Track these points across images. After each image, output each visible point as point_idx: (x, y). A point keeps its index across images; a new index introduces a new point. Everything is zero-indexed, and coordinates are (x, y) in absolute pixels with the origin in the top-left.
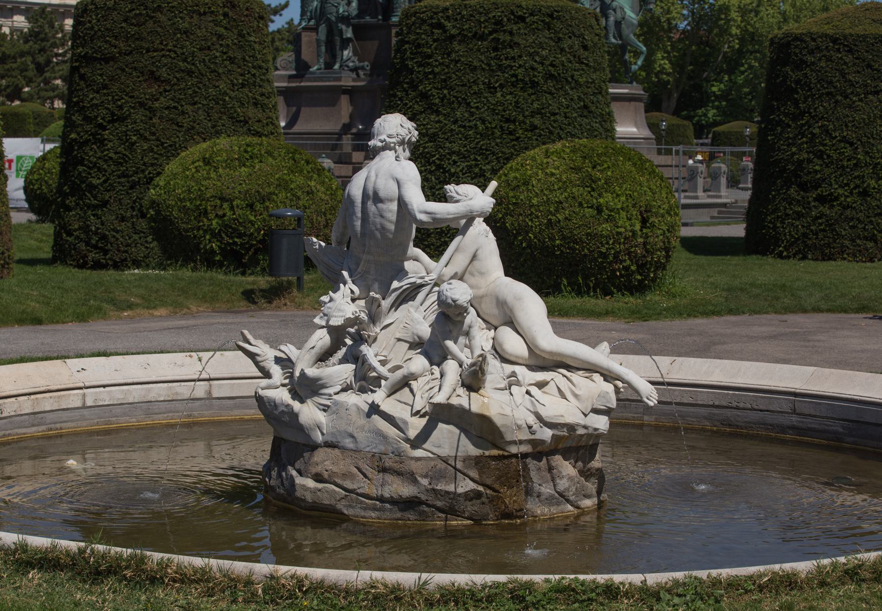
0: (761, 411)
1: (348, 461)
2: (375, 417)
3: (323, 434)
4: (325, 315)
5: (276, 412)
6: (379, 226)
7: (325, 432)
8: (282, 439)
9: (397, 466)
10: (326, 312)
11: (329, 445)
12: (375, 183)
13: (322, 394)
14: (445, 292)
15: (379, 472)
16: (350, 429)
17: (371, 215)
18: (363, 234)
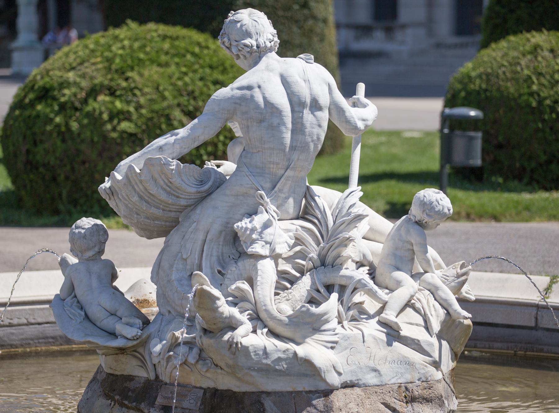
0: (39, 324)
1: (374, 398)
2: (396, 344)
3: (340, 374)
4: (267, 243)
5: (268, 362)
6: (315, 138)
7: (342, 372)
8: (263, 392)
9: (426, 393)
10: (269, 239)
11: (346, 386)
12: (311, 89)
13: (324, 331)
14: (440, 202)
15: (407, 403)
16: (371, 364)
17: (308, 125)
18: (293, 148)
